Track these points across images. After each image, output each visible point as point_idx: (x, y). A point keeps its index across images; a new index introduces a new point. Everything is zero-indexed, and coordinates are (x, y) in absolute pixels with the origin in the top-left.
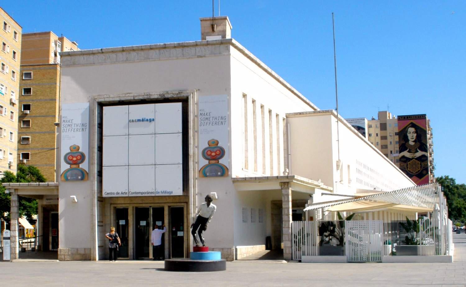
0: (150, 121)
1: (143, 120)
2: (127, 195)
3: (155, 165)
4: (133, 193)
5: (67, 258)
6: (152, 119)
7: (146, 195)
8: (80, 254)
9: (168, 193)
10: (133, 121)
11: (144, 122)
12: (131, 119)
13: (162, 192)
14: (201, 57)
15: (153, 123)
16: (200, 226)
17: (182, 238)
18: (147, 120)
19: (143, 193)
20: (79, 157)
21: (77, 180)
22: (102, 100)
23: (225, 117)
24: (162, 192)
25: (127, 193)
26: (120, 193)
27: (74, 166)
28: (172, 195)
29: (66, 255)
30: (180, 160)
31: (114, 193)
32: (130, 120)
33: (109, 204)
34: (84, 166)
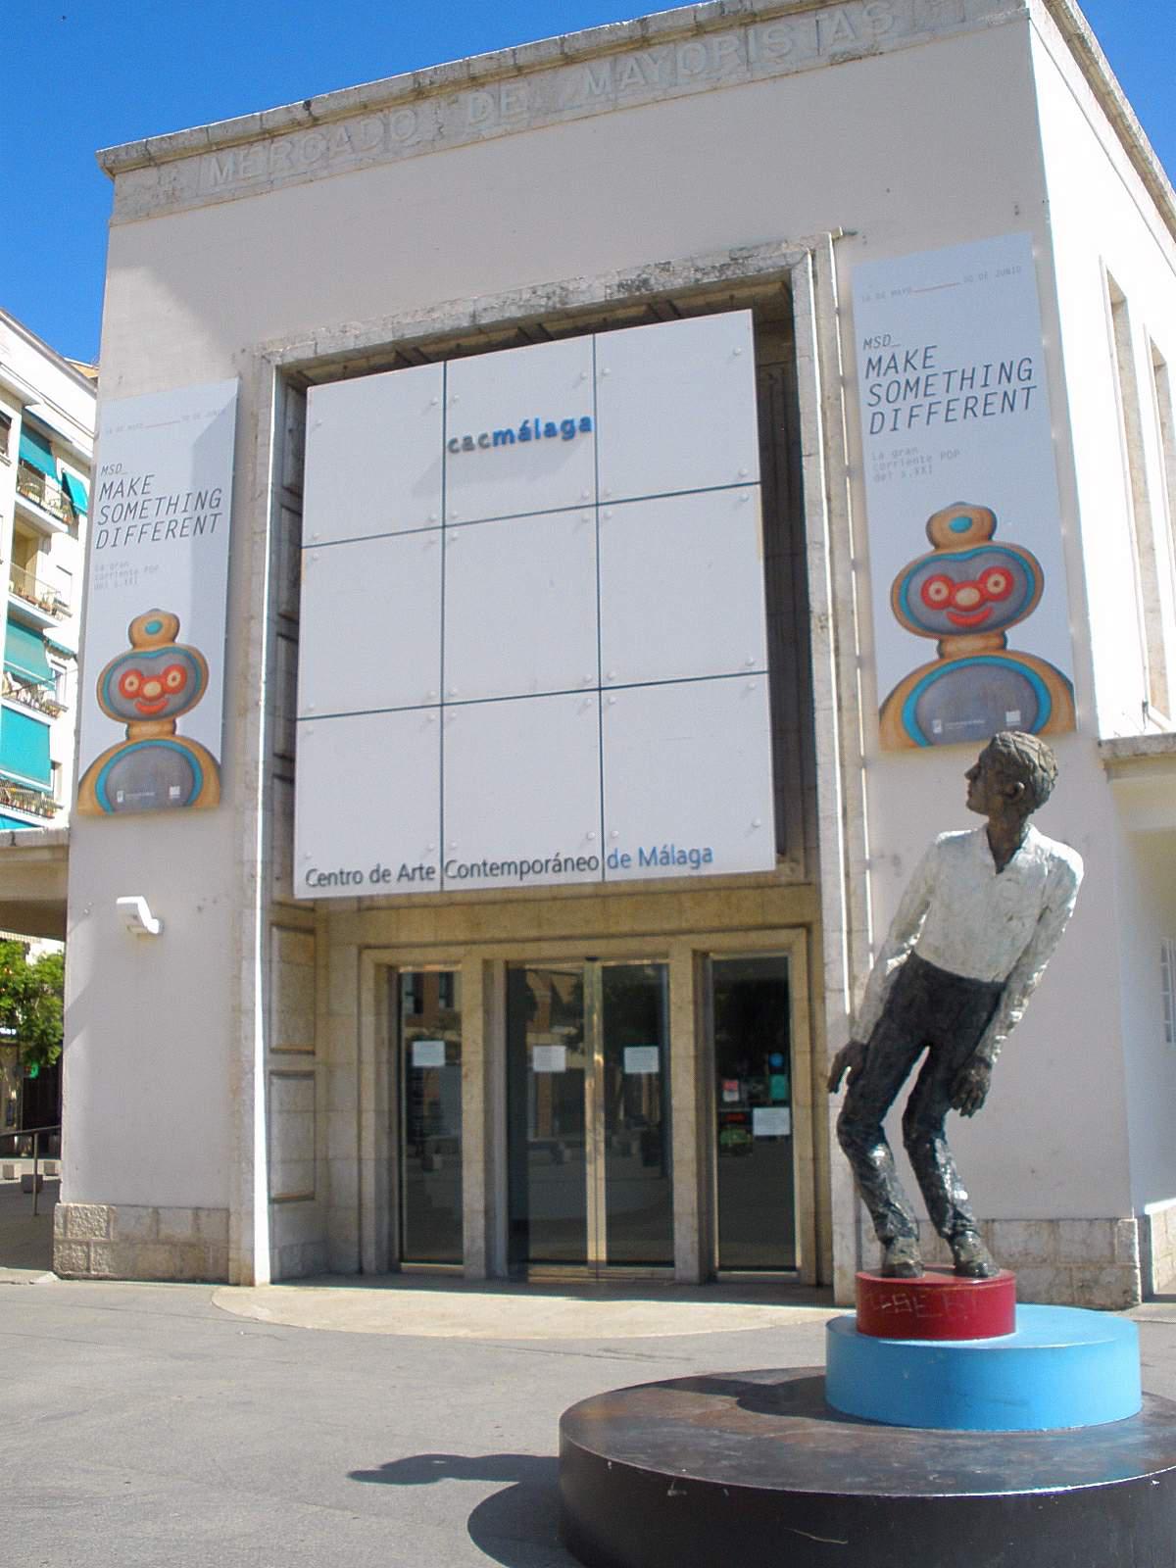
0: (569, 431)
1: (525, 435)
2: (433, 886)
3: (600, 689)
4: (470, 871)
5: (102, 1261)
6: (577, 424)
7: (548, 879)
8: (169, 1242)
9: (683, 859)
10: (468, 444)
11: (533, 443)
12: (456, 432)
13: (647, 854)
15: (583, 442)
16: (917, 1067)
17: (781, 1146)
18: (550, 431)
19: (531, 868)
20: (174, 679)
21: (164, 806)
22: (299, 352)
23: (1026, 365)
24: (647, 854)
25: (430, 871)
26: (395, 872)
27: (148, 730)
28: (707, 870)
29: (97, 1244)
30: (756, 650)
31: (355, 877)
33: (354, 950)
34: (200, 725)
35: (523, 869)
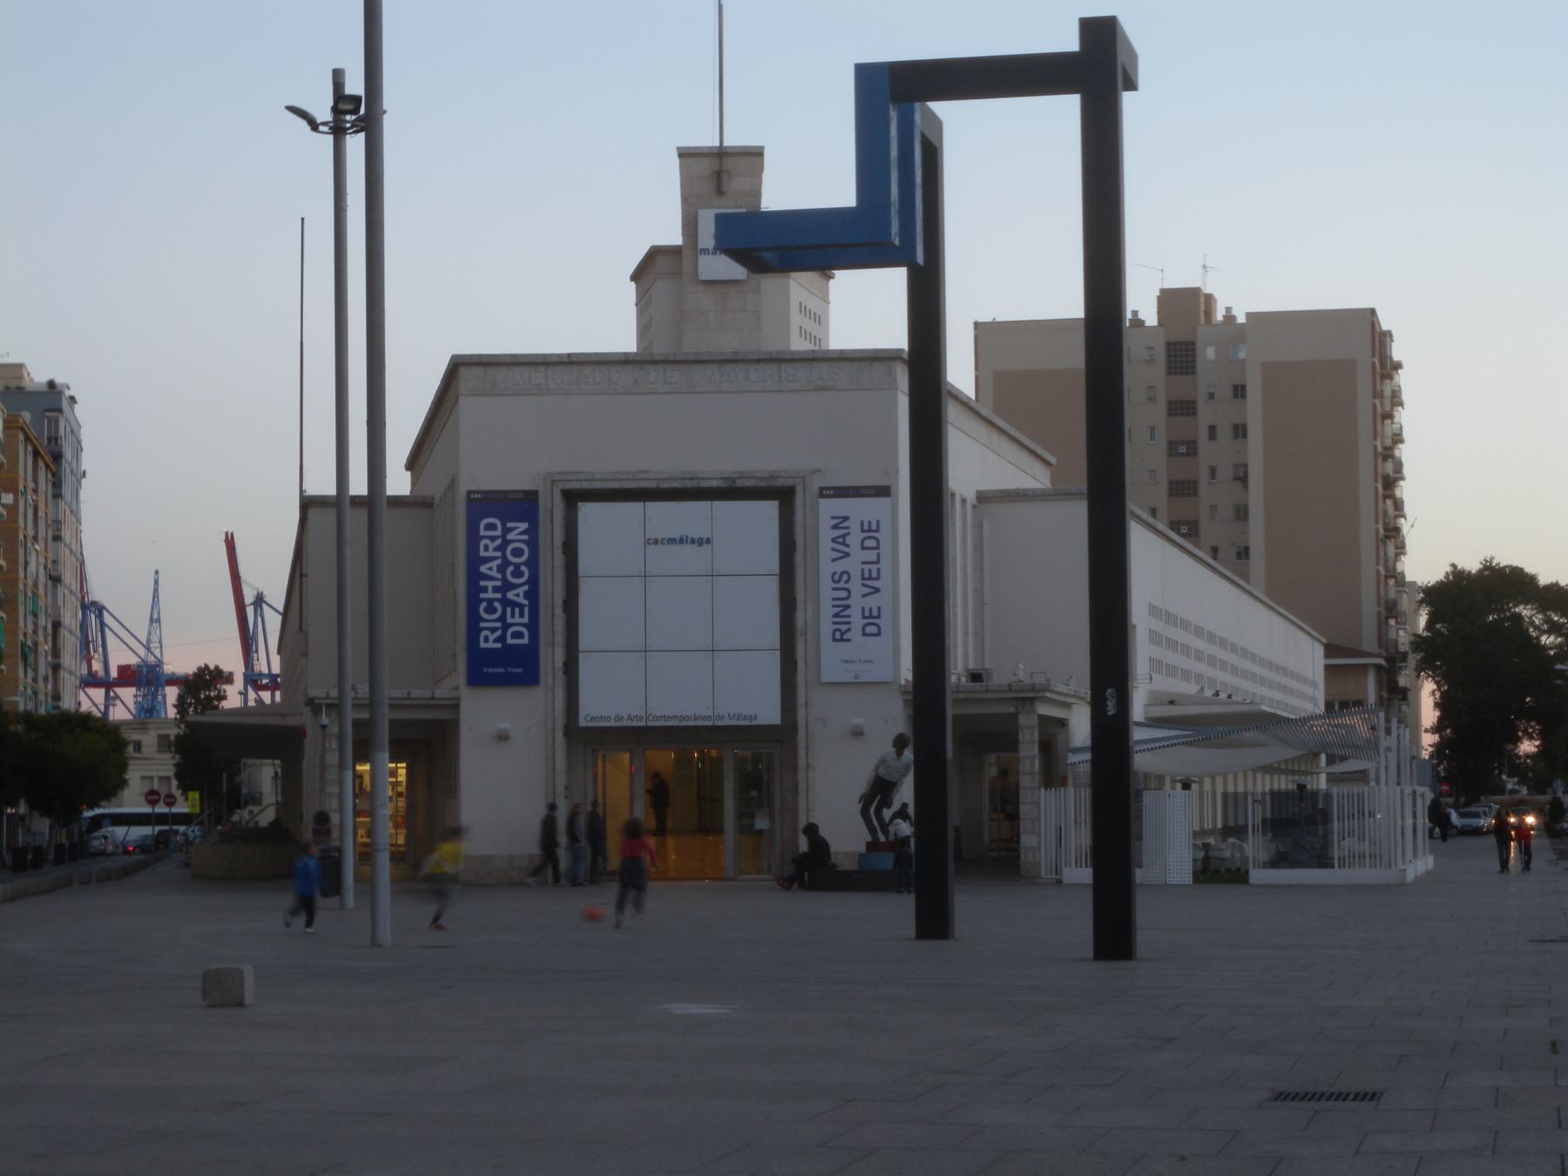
1: (681, 541)
2: (643, 724)
4: (656, 718)
10: (656, 542)
13: (731, 715)
14: (823, 389)
18: (693, 541)
28: (754, 723)
32: (650, 539)
35: (682, 718)
